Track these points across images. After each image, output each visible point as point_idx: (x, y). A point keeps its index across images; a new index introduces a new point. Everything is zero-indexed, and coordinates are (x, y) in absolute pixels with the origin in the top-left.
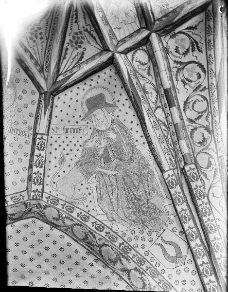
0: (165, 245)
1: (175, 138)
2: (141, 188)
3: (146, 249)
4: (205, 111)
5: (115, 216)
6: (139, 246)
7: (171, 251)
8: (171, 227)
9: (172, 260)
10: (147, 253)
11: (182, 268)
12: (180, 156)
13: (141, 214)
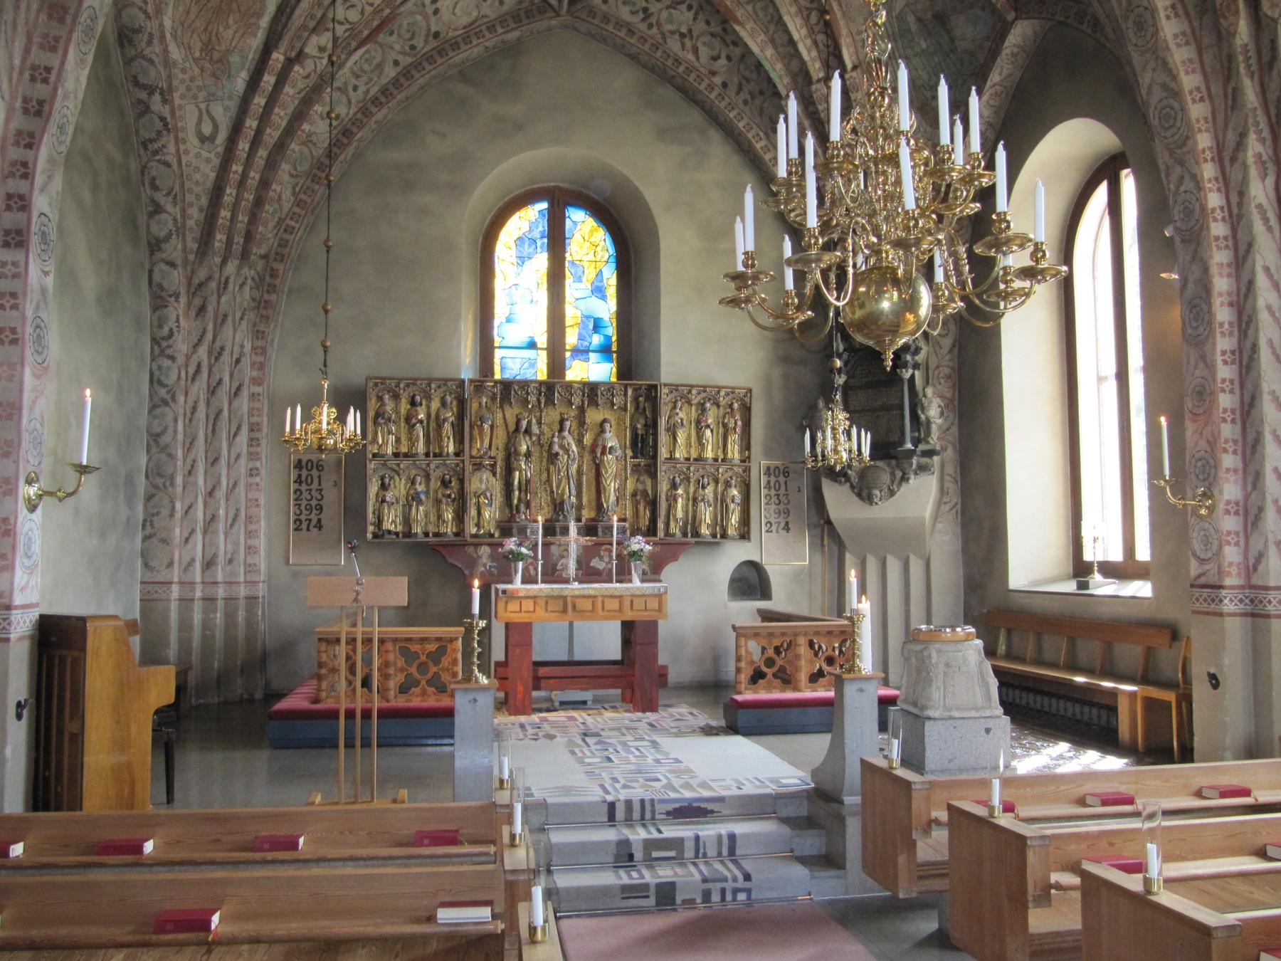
0: (205, 116)
1: (312, 24)
2: (231, 32)
3: (182, 102)
4: (351, 23)
5: (179, 33)
6: (179, 94)
7: (207, 130)
8: (227, 103)
9: (203, 139)
10: (181, 107)
11: (205, 154)
12: (298, 45)
13: (208, 58)
